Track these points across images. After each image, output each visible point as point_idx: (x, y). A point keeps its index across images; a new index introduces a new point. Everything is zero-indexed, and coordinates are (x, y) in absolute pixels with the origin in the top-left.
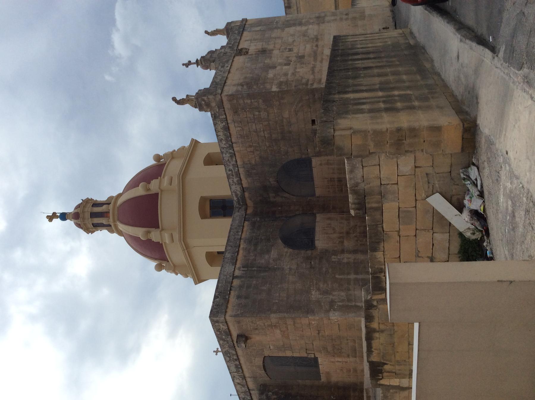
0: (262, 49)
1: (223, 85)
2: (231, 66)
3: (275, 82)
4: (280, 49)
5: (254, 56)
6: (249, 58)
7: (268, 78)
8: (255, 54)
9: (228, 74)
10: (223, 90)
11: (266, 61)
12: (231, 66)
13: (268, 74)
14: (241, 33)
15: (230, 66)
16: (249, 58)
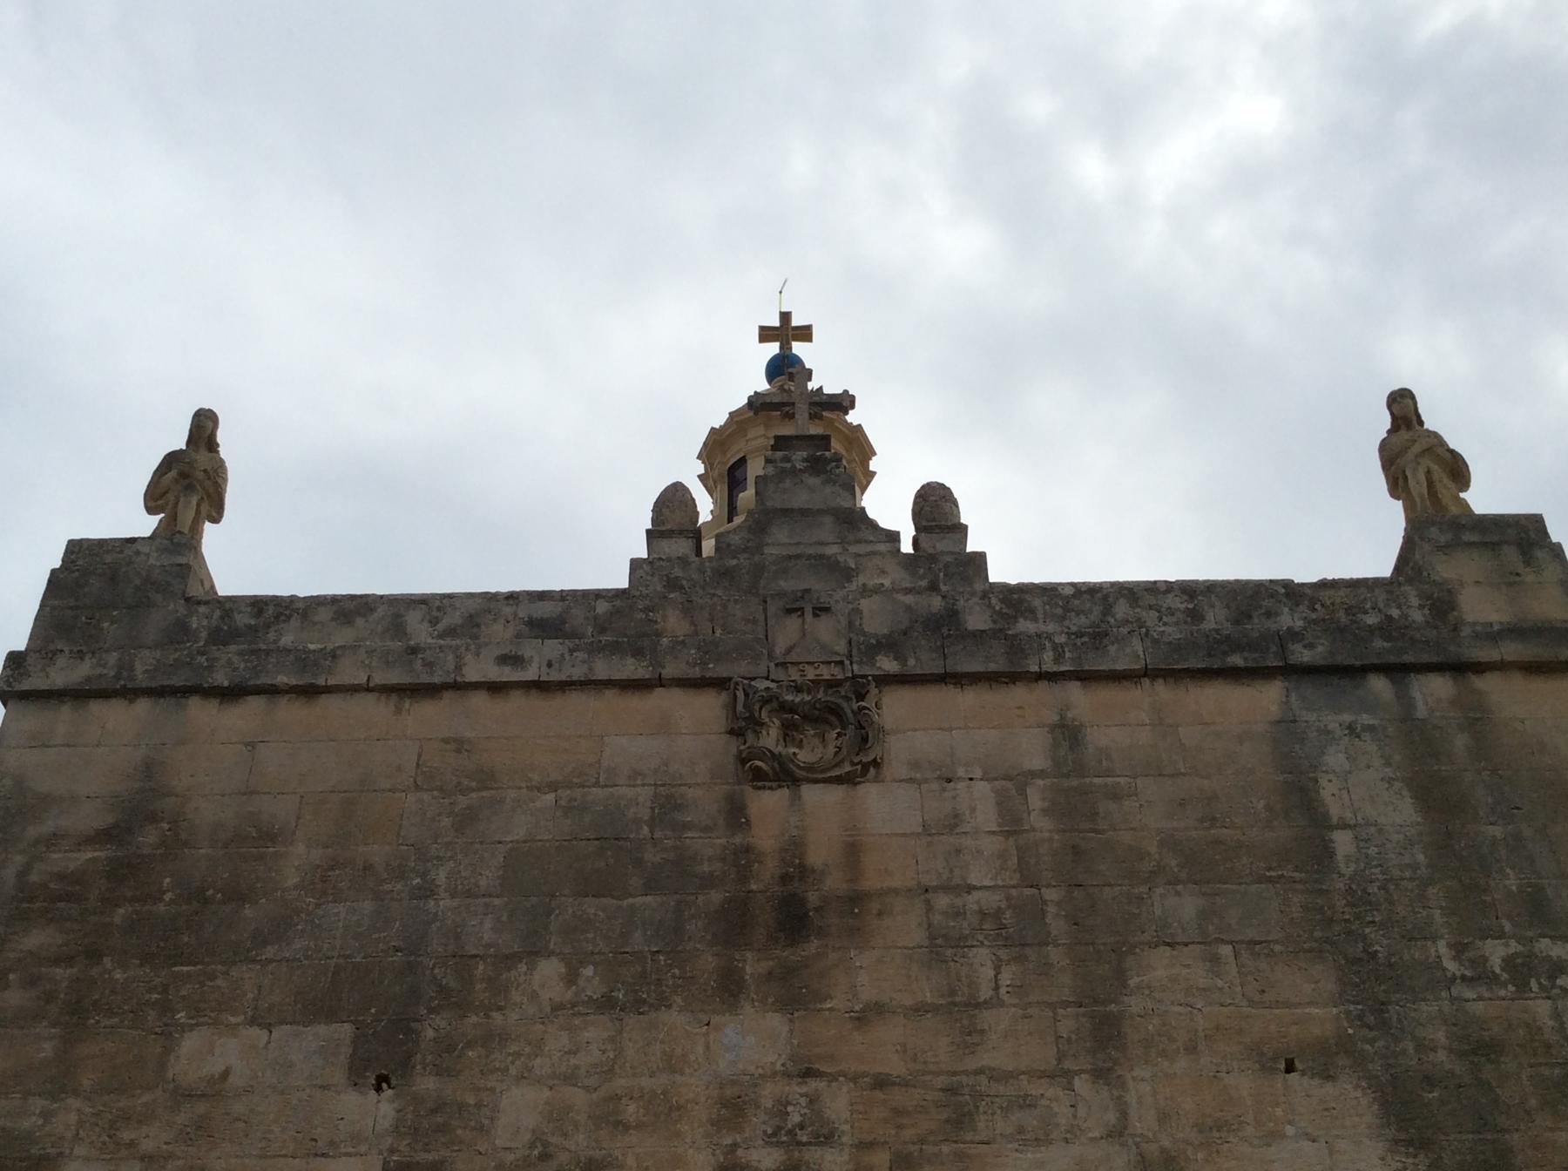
0: (856, 900)
1: (177, 681)
2: (539, 686)
3: (46, 1115)
4: (808, 1073)
5: (709, 847)
6: (668, 806)
7: (169, 1036)
8: (743, 859)
9: (388, 690)
10: (104, 694)
11: (549, 970)
12: (539, 686)
13: (252, 1022)
14: (1237, 660)
15: (530, 674)
16: (668, 806)
